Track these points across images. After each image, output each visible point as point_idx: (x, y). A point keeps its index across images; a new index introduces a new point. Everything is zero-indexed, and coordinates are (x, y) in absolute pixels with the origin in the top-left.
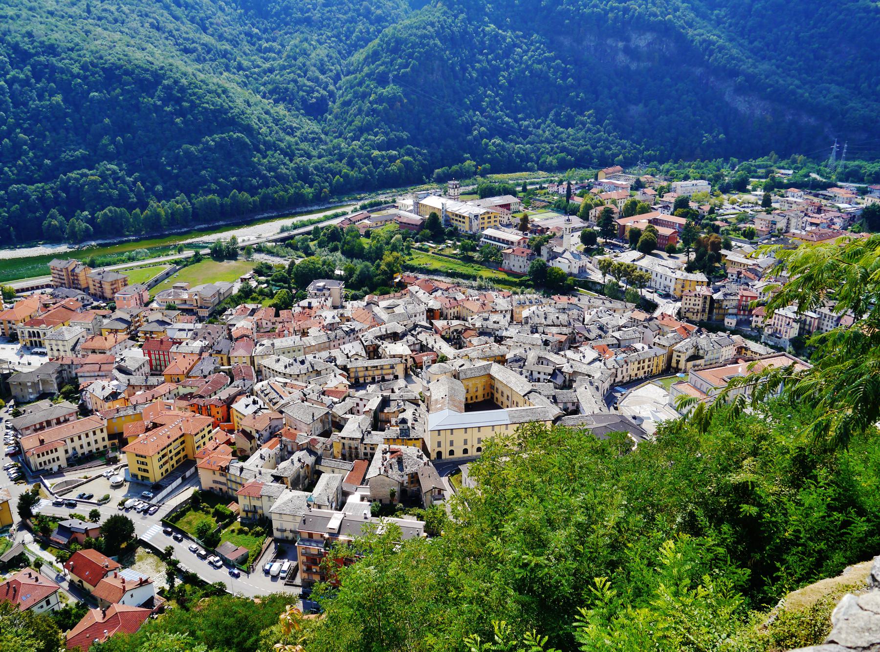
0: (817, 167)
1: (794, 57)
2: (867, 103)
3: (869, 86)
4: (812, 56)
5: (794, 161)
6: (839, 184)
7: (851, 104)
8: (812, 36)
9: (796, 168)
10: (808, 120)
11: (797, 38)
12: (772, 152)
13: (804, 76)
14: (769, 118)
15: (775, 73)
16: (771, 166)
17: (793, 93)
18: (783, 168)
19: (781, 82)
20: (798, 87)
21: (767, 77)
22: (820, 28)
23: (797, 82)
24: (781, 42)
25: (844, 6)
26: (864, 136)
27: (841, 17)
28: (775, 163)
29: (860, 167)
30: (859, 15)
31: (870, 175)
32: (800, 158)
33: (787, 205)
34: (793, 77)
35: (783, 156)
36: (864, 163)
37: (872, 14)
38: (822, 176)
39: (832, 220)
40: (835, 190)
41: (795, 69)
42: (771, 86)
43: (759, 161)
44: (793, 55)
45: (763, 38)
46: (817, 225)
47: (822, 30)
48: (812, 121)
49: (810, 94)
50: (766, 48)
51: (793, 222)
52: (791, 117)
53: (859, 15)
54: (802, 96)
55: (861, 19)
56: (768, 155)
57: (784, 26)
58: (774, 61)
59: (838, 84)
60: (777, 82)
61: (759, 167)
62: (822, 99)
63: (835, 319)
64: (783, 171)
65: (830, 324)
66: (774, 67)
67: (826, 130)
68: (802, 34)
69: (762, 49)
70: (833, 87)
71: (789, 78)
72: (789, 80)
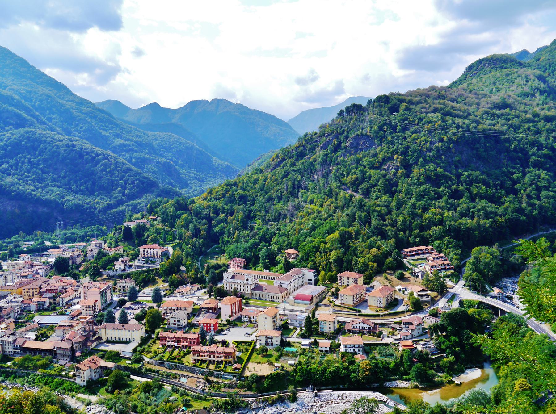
0: (49, 236)
1: (29, 173)
2: (76, 196)
3: (77, 187)
4: (40, 172)
5: (36, 236)
6: (60, 245)
7: (68, 198)
8: (39, 161)
9: (37, 240)
10: (42, 210)
11: (30, 162)
12: (21, 232)
13: (37, 183)
14: (17, 211)
15: (17, 184)
16: (20, 241)
17: (30, 194)
18: (29, 241)
19: (21, 188)
20: (34, 191)
21: (11, 186)
22: (42, 156)
23: (33, 188)
24: (20, 164)
25: (54, 144)
26: (78, 215)
27: (54, 149)
28: (24, 238)
29: (73, 234)
30: (63, 148)
31: (80, 237)
32: (38, 233)
33: (11, 267)
34: (30, 184)
35: (29, 231)
36: (77, 230)
37: (71, 148)
38: (52, 242)
39: (37, 271)
40: (52, 250)
41: (30, 180)
42: (14, 191)
43: (13, 239)
44: (29, 172)
45: (8, 162)
46: (26, 277)
47: (44, 157)
48: (45, 209)
49: (41, 194)
50: (10, 168)
51: (9, 278)
52: (31, 209)
53: (63, 148)
54: (35, 196)
55: (65, 150)
56: (18, 234)
57: (20, 155)
58: (16, 176)
59: (59, 187)
60: (18, 188)
61: (9, 243)
62: (49, 196)
63: (12, 342)
64: (28, 243)
65: (10, 347)
66: (16, 180)
67: (55, 214)
68: (32, 160)
69: (8, 170)
70: (55, 189)
71: (26, 186)
72: (27, 187)
